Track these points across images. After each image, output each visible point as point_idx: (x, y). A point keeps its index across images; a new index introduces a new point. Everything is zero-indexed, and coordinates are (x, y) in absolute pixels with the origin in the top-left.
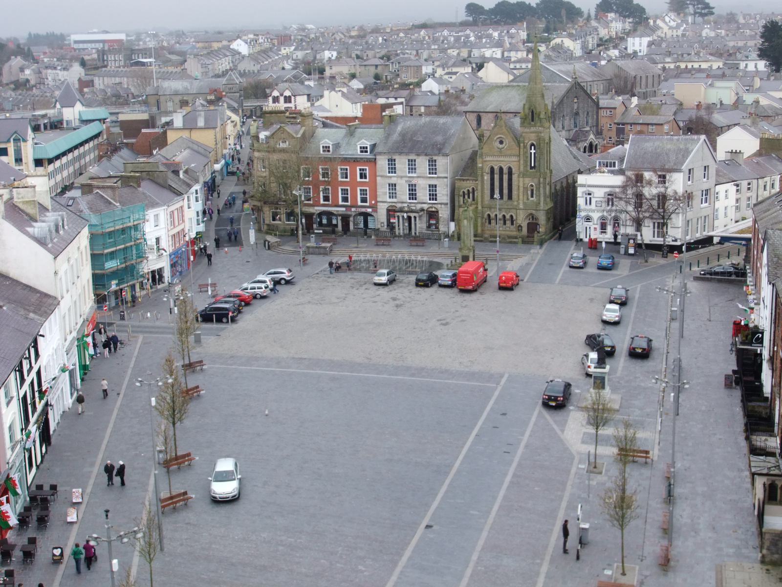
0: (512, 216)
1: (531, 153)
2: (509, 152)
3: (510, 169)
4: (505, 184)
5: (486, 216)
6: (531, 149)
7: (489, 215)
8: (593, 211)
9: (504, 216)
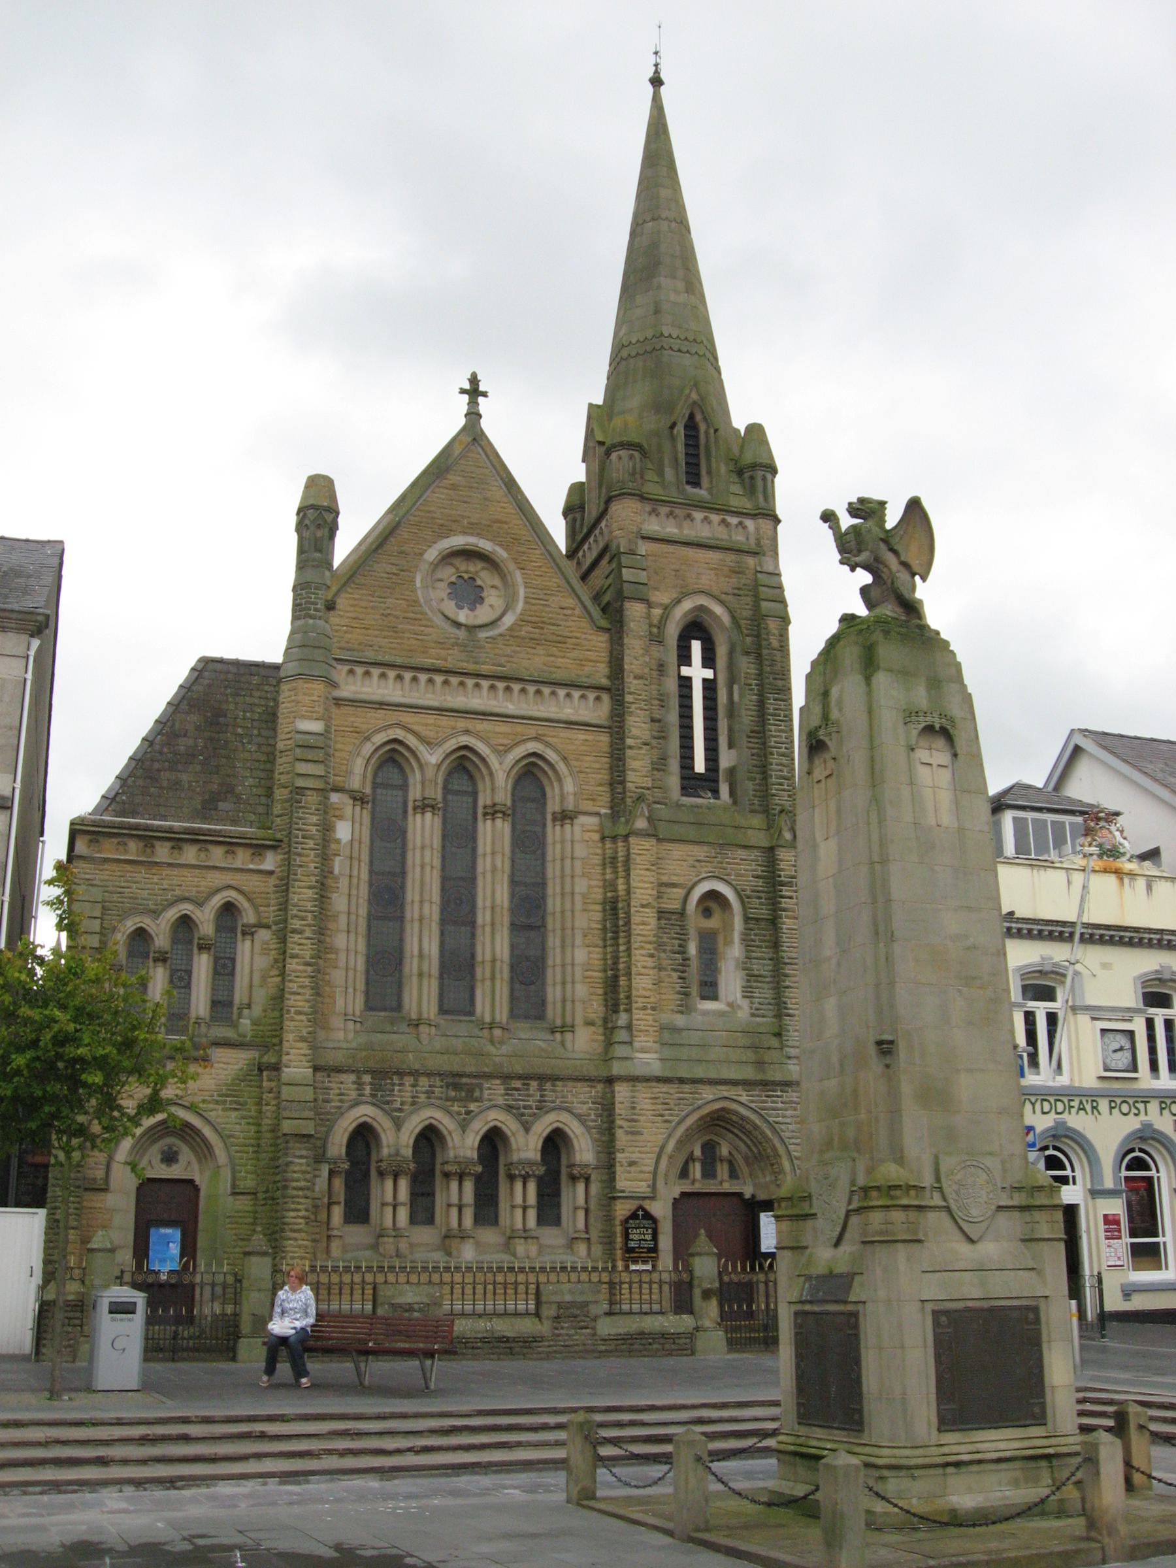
0: (555, 1142)
1: (686, 683)
2: (534, 661)
3: (532, 775)
4: (494, 893)
5: (338, 1144)
6: (685, 658)
7: (364, 1135)
9: (493, 1141)
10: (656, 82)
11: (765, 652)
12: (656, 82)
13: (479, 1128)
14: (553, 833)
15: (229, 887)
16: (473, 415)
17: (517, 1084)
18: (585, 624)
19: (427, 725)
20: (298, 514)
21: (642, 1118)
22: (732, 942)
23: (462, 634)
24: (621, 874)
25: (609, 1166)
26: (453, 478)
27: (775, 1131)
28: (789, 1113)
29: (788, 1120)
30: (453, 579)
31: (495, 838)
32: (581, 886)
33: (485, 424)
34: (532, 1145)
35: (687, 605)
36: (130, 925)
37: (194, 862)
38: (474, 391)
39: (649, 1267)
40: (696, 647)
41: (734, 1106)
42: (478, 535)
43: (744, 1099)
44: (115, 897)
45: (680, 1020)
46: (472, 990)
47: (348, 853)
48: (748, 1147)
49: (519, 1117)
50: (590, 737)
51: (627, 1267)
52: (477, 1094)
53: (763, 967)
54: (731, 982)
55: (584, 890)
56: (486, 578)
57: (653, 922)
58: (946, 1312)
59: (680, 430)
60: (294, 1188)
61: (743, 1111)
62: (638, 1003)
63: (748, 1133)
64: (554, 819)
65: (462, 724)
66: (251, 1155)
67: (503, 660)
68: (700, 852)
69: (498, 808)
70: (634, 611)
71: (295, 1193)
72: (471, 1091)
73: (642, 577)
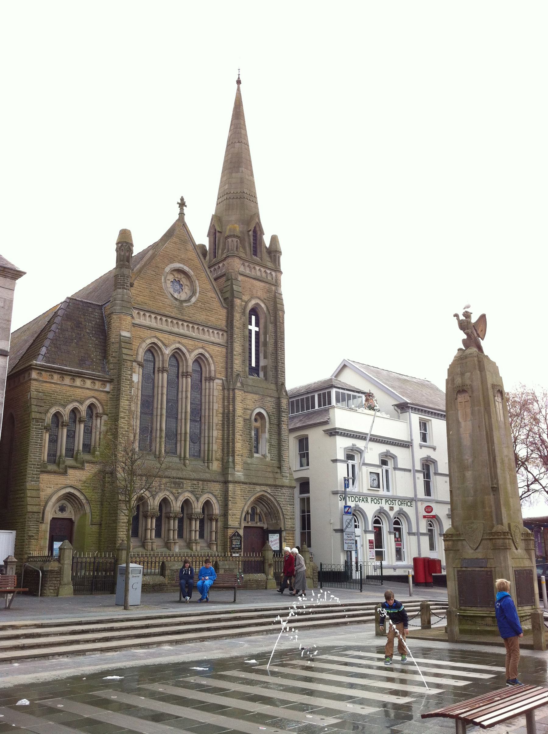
2: (201, 317)
8: (364, 498)
10: (239, 82)
11: (278, 323)
12: (239, 82)
13: (182, 499)
14: (205, 385)
15: (93, 397)
16: (182, 214)
17: (195, 482)
18: (219, 304)
19: (165, 338)
20: (117, 244)
21: (237, 497)
22: (265, 432)
23: (177, 303)
24: (231, 403)
25: (225, 515)
26: (174, 239)
27: (279, 504)
28: (283, 497)
29: (282, 500)
30: (172, 280)
31: (186, 383)
32: (216, 406)
33: (187, 219)
34: (199, 507)
35: (253, 302)
36: (53, 411)
37: (90, 387)
38: (182, 204)
39: (238, 555)
40: (253, 318)
41: (266, 494)
42: (184, 264)
43: (269, 491)
44: (48, 398)
45: (249, 461)
46: (176, 444)
47: (136, 387)
48: (267, 509)
49: (195, 495)
50: (220, 349)
51: (231, 555)
52: (181, 485)
53: (274, 442)
54: (264, 447)
55: (217, 408)
56: (184, 281)
57: (242, 422)
58: (517, 571)
59: (251, 233)
60: (123, 523)
61: (268, 495)
62: (237, 453)
63: (268, 504)
64: (206, 380)
65: (178, 339)
66: (99, 508)
67: (191, 315)
68: (256, 397)
69: (189, 374)
70: (237, 302)
71: (123, 524)
72: (179, 484)
73: (240, 289)
